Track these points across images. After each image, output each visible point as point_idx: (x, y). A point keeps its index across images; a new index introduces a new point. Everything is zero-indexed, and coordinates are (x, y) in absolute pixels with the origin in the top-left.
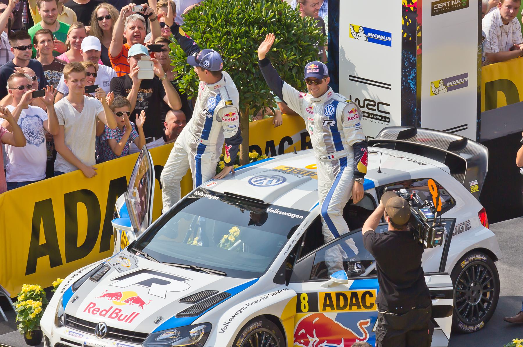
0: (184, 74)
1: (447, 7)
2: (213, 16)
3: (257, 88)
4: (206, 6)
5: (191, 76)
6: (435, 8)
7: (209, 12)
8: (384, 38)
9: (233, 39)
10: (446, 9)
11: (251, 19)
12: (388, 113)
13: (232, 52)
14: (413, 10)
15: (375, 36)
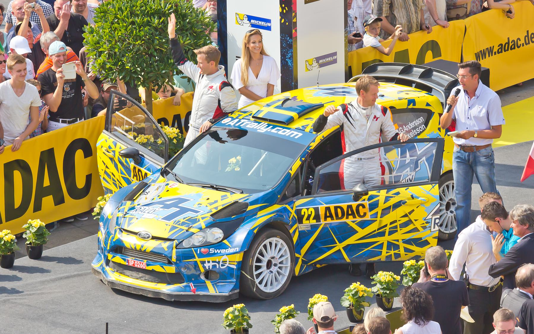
0: (95, 59)
2: (120, 9)
5: (103, 60)
8: (265, 24)
9: (137, 28)
11: (152, 11)
13: (136, 39)
15: (257, 23)
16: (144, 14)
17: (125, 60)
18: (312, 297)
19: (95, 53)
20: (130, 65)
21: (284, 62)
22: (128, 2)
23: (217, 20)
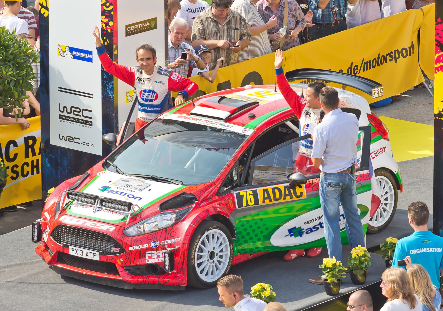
1: (139, 29)
6: (128, 30)
8: (86, 56)
10: (138, 30)
12: (91, 118)
21: (105, 94)
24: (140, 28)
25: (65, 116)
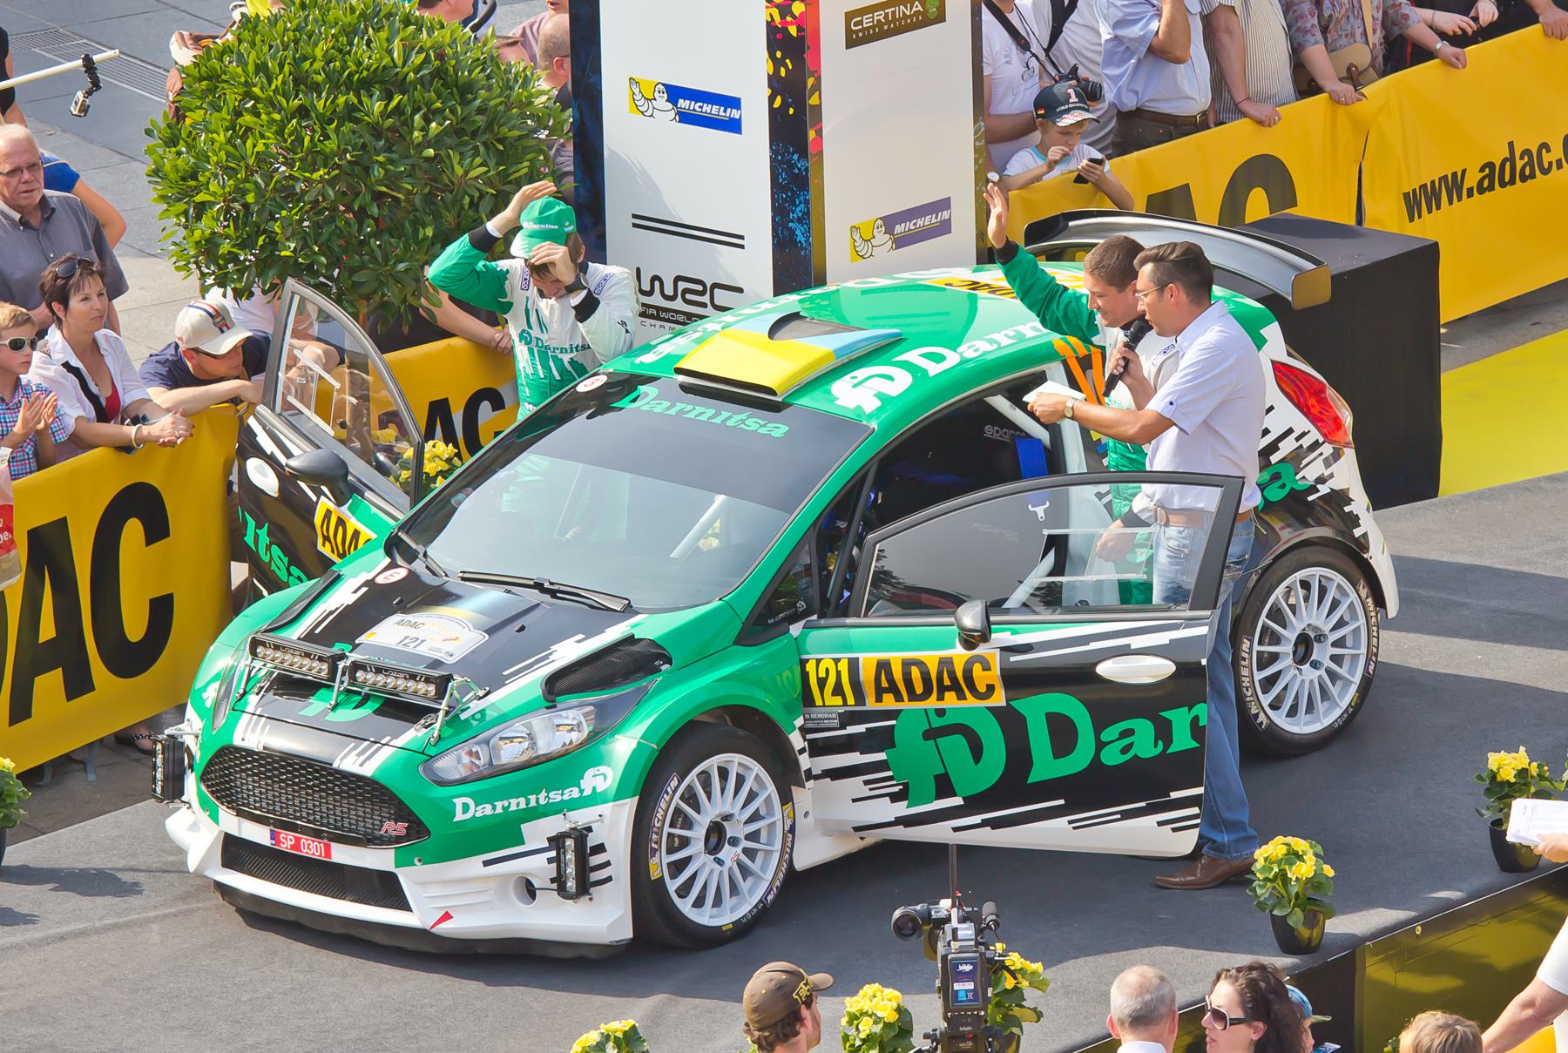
2: (261, 68)
3: (386, 259)
4: (240, 41)
5: (209, 231)
6: (854, 28)
7: (248, 56)
8: (721, 113)
9: (317, 127)
10: (886, 27)
11: (362, 73)
13: (314, 163)
14: (795, 35)
16: (336, 83)
17: (278, 230)
18: (854, 993)
19: (181, 206)
20: (293, 246)
22: (288, 46)
23: (572, 100)
24: (891, 22)
25: (658, 309)
